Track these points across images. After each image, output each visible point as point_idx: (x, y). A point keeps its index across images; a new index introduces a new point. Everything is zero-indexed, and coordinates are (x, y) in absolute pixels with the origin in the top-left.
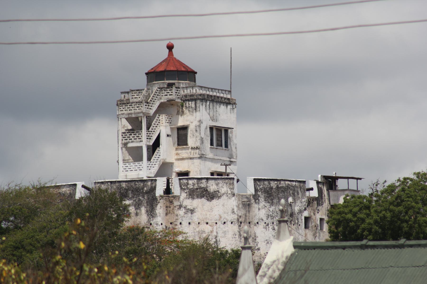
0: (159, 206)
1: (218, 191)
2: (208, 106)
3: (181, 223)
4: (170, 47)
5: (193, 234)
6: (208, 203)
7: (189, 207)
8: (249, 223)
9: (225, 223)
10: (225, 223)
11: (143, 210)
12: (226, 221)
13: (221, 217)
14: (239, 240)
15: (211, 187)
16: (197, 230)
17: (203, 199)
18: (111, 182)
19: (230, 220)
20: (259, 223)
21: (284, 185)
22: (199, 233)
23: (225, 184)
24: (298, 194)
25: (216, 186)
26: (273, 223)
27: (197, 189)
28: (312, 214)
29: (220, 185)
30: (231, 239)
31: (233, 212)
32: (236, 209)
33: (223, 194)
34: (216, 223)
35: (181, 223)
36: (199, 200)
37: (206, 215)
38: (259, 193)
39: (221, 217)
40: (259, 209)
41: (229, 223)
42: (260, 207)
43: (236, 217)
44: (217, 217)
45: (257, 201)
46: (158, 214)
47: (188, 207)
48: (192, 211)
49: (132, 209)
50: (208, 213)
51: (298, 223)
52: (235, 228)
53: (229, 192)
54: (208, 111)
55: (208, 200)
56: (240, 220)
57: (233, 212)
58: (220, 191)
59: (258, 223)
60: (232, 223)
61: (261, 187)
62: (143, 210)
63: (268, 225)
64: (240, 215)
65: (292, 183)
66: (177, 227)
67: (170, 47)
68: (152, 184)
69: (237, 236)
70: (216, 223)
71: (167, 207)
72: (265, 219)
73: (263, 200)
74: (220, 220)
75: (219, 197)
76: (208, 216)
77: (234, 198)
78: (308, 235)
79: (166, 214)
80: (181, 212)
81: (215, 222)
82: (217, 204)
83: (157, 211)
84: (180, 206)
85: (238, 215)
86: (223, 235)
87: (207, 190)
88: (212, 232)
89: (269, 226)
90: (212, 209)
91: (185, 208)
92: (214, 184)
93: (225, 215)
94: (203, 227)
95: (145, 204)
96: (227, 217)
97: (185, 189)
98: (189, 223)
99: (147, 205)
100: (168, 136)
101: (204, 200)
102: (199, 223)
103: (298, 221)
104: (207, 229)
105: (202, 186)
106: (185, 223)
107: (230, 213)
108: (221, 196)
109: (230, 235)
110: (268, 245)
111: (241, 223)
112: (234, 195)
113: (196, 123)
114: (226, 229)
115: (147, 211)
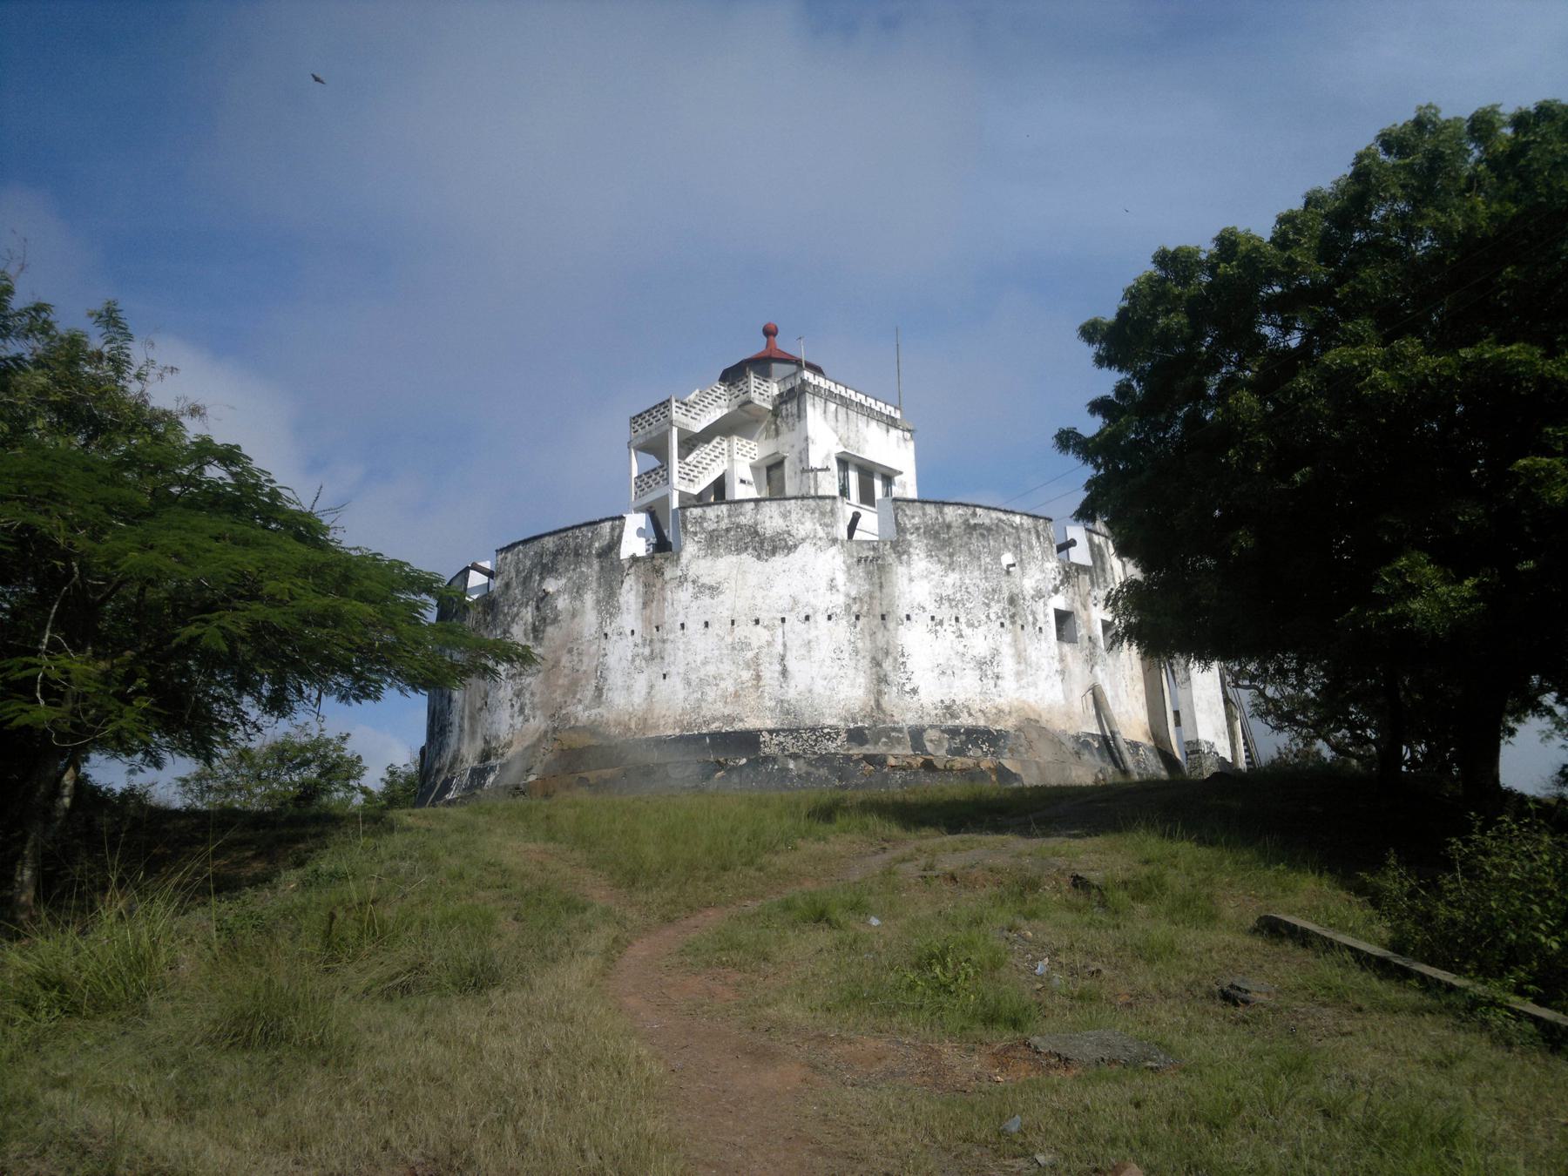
0: (626, 586)
1: (789, 533)
2: (831, 415)
3: (683, 626)
4: (770, 332)
5: (716, 653)
6: (759, 565)
7: (705, 580)
8: (883, 617)
9: (807, 618)
10: (807, 618)
11: (589, 598)
12: (810, 612)
13: (795, 601)
14: (853, 663)
15: (768, 524)
16: (729, 640)
17: (744, 556)
18: (525, 542)
19: (822, 607)
20: (913, 617)
21: (987, 522)
22: (734, 648)
23: (808, 514)
24: (1031, 548)
25: (781, 521)
26: (957, 619)
27: (728, 530)
28: (1078, 605)
29: (794, 517)
30: (828, 662)
31: (832, 586)
32: (841, 579)
33: (803, 540)
34: (783, 620)
35: (683, 626)
36: (733, 559)
37: (754, 597)
38: (909, 537)
39: (795, 601)
40: (911, 580)
41: (821, 619)
42: (914, 573)
43: (840, 599)
44: (786, 603)
45: (905, 557)
46: (624, 608)
47: (702, 580)
48: (714, 590)
49: (562, 603)
50: (759, 594)
51: (1034, 624)
52: (842, 630)
53: (821, 533)
54: (833, 423)
55: (759, 557)
56: (855, 608)
57: (832, 586)
58: (794, 532)
59: (908, 617)
60: (830, 618)
61: (916, 520)
62: (589, 598)
63: (941, 623)
64: (853, 594)
65: (1010, 516)
66: (671, 637)
67: (770, 332)
68: (613, 529)
69: (846, 655)
70: (783, 620)
71: (646, 585)
72: (931, 608)
73: (922, 555)
74: (792, 610)
75: (790, 549)
76: (759, 601)
77: (834, 550)
78: (1069, 659)
79: (645, 605)
80: (684, 595)
81: (780, 616)
82: (786, 567)
83: (622, 600)
84: (682, 580)
85: (848, 595)
86: (803, 651)
87: (756, 532)
88: (769, 644)
89: (946, 626)
90: (768, 583)
91: (694, 582)
92: (776, 515)
93: (810, 597)
94: (744, 630)
95: (594, 585)
96: (813, 601)
97: (695, 534)
98: (707, 624)
99: (600, 586)
100: (742, 481)
101: (747, 559)
102: (733, 622)
103: (1035, 620)
104: (759, 636)
105: (743, 520)
106: (694, 626)
107: (822, 591)
108: (796, 546)
109: (824, 650)
110: (944, 679)
111: (857, 618)
112: (834, 541)
113: (799, 446)
114: (813, 633)
115: (598, 602)
